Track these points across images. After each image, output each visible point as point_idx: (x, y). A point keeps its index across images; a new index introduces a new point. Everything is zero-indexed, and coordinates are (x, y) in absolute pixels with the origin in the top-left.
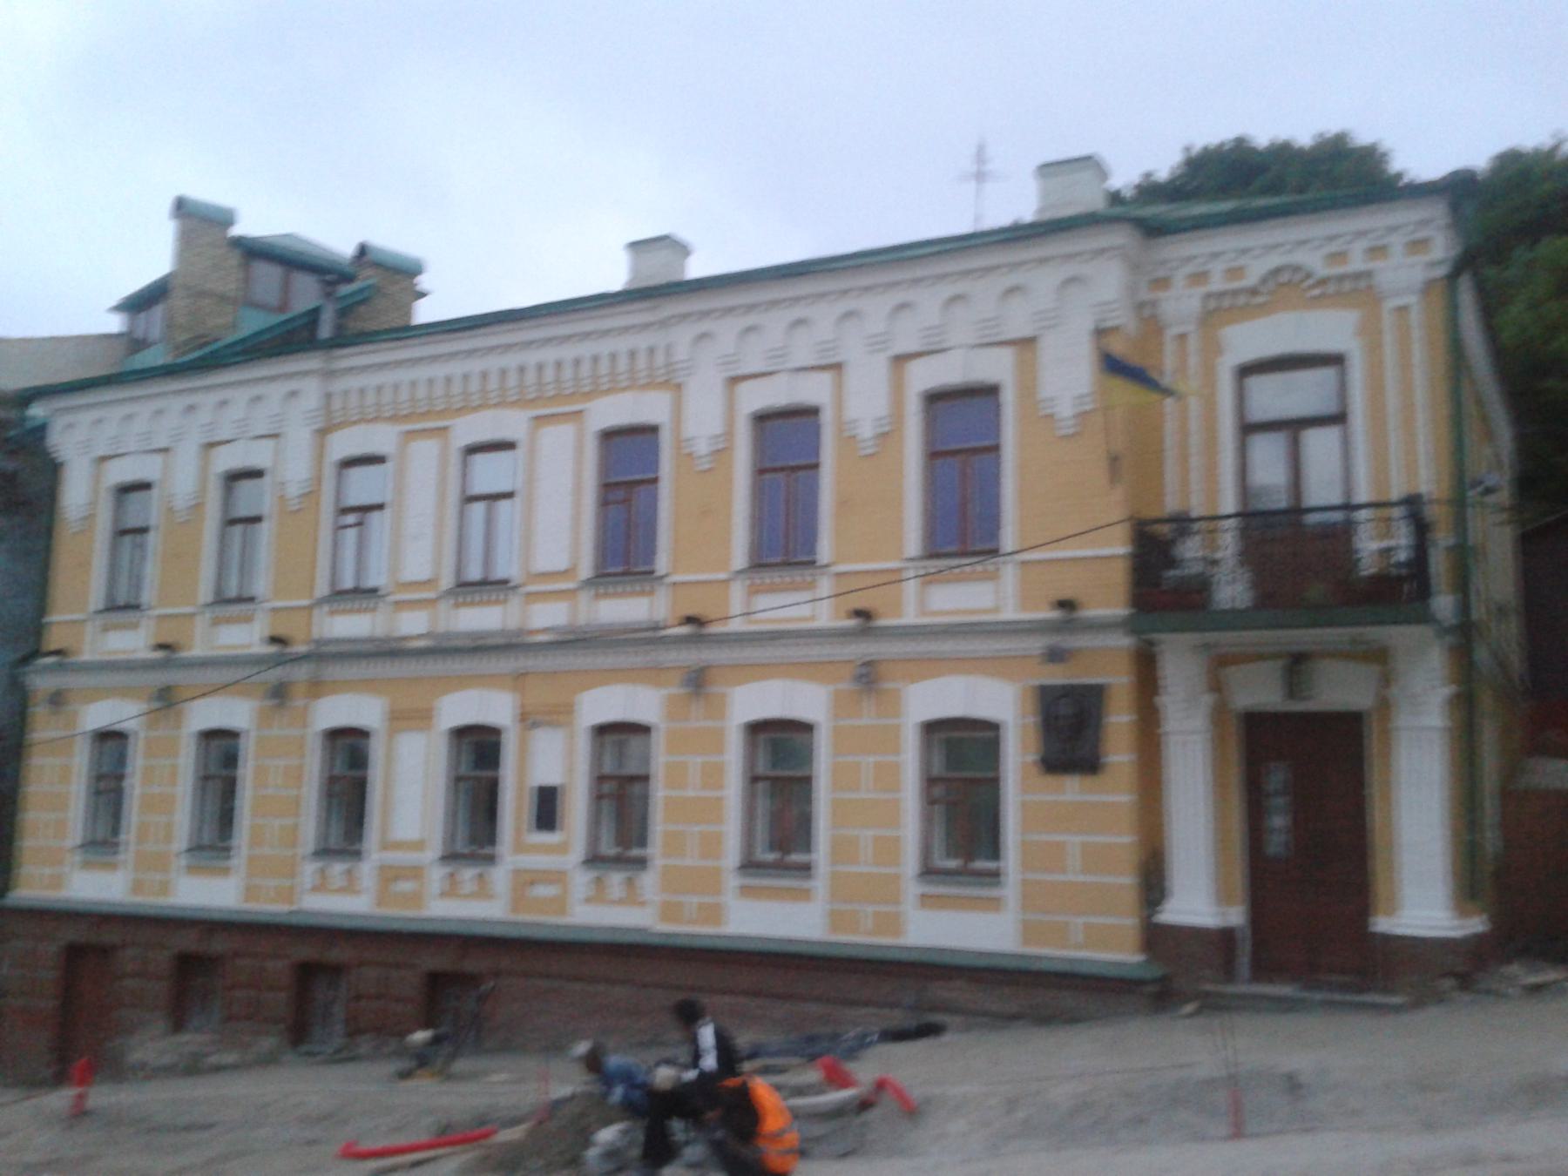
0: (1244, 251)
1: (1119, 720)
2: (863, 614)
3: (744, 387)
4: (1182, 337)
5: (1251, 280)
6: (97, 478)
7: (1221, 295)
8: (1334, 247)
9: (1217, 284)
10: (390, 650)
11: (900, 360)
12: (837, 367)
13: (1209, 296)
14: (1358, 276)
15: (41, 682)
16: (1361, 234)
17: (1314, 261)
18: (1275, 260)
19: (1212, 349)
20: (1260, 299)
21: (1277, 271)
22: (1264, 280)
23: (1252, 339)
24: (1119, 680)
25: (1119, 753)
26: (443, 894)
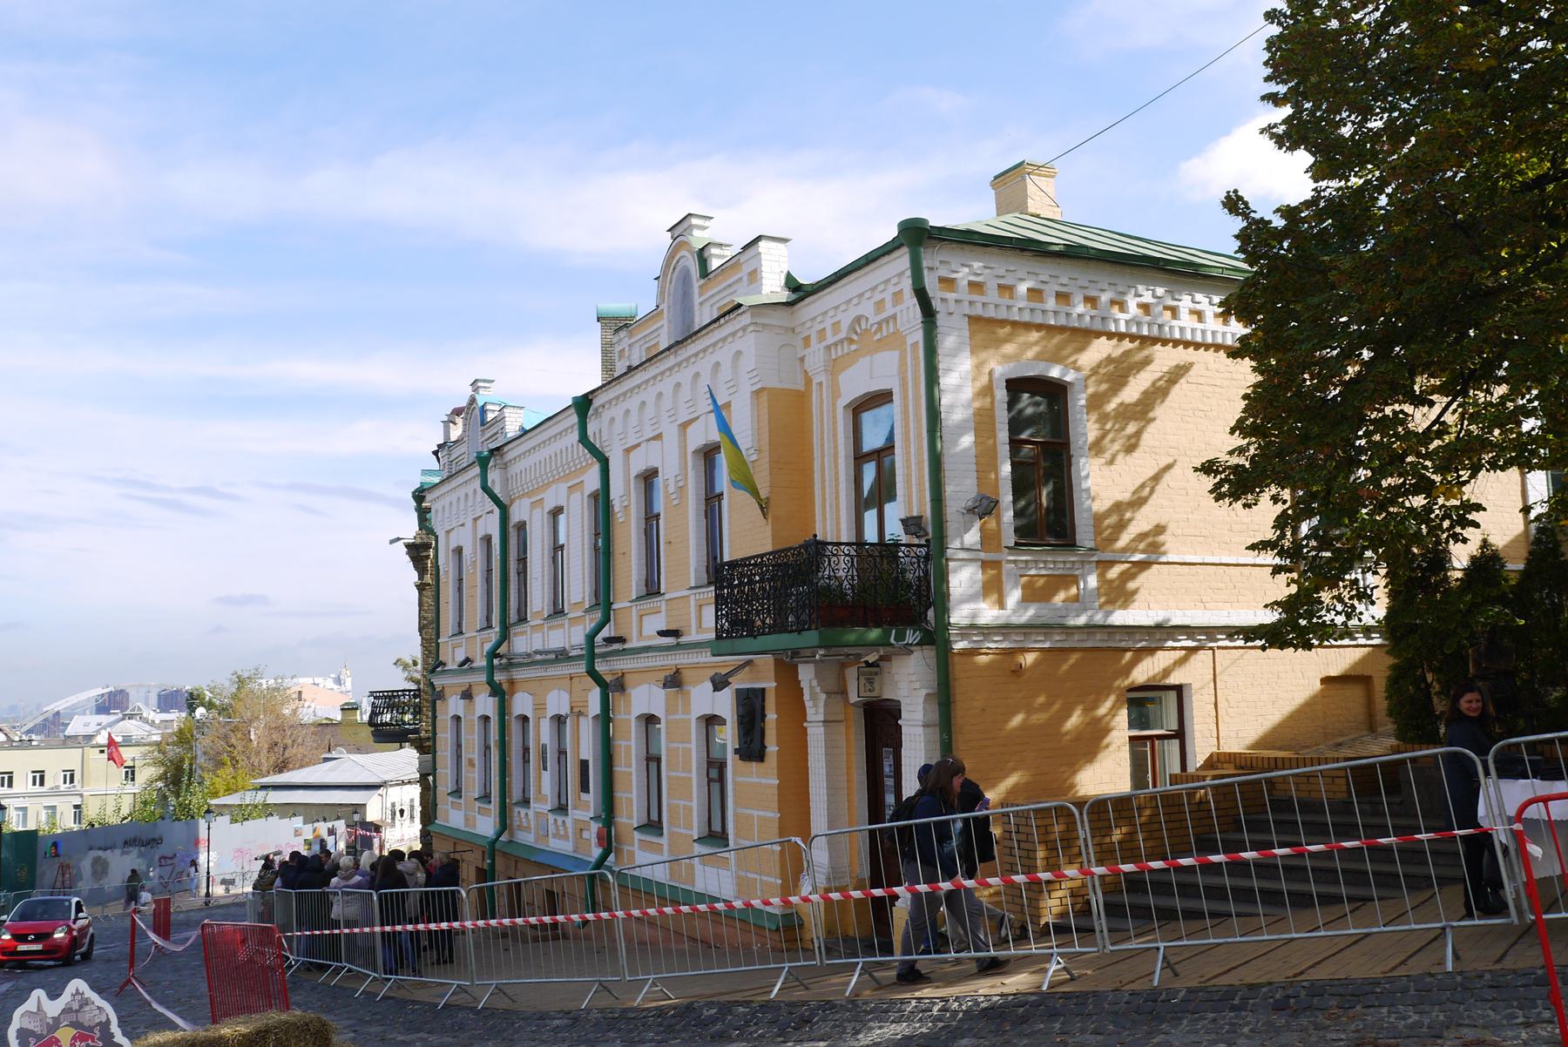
0: (836, 308)
1: (771, 716)
2: (675, 633)
3: (633, 454)
4: (820, 384)
5: (843, 335)
6: (447, 543)
7: (836, 344)
8: (878, 297)
9: (830, 340)
10: (530, 661)
11: (684, 426)
12: (658, 437)
13: (828, 348)
14: (894, 317)
15: (438, 682)
16: (887, 282)
17: (867, 309)
18: (854, 312)
19: (836, 393)
20: (853, 347)
21: (858, 319)
22: (852, 329)
23: (856, 384)
24: (770, 685)
25: (772, 748)
26: (555, 836)
